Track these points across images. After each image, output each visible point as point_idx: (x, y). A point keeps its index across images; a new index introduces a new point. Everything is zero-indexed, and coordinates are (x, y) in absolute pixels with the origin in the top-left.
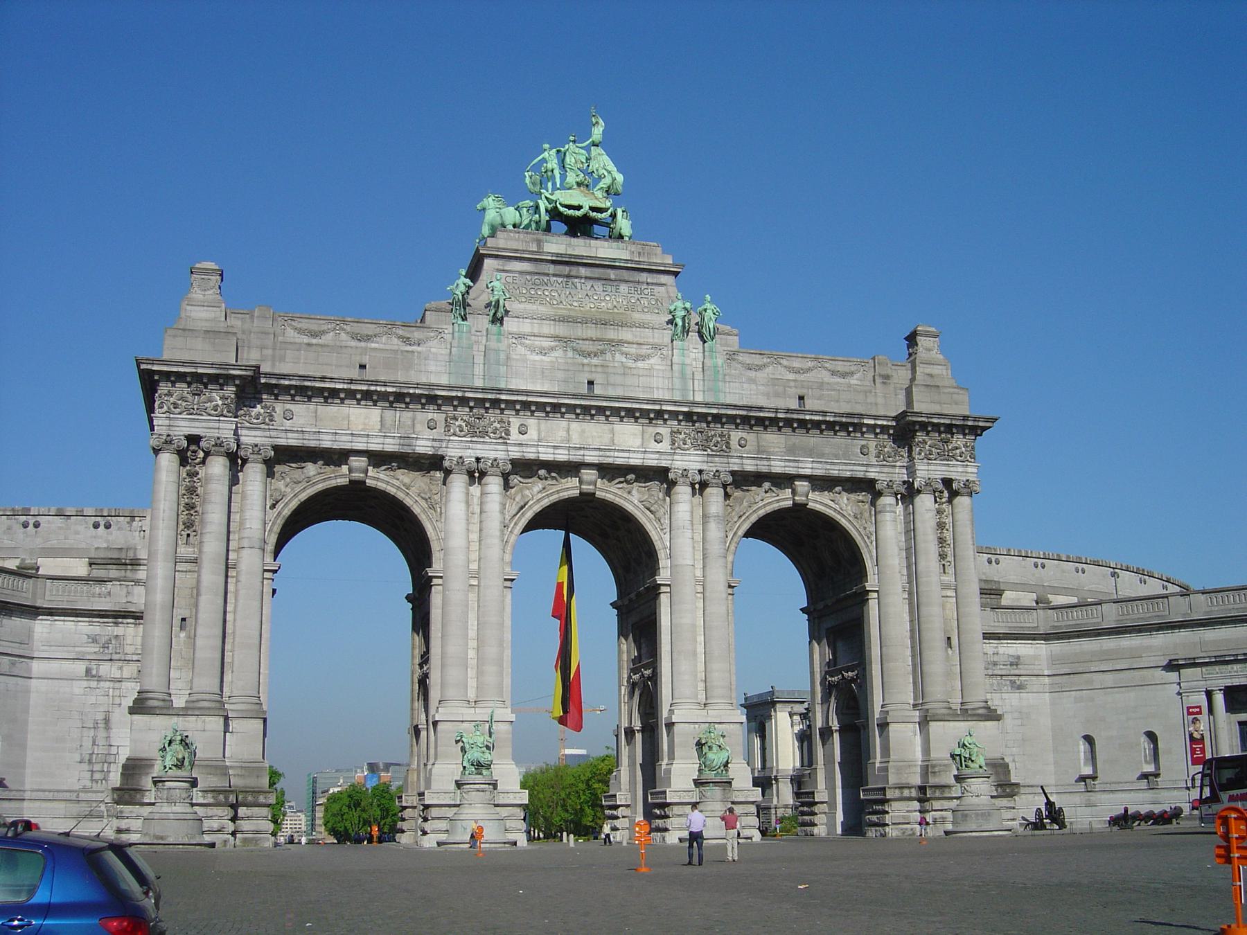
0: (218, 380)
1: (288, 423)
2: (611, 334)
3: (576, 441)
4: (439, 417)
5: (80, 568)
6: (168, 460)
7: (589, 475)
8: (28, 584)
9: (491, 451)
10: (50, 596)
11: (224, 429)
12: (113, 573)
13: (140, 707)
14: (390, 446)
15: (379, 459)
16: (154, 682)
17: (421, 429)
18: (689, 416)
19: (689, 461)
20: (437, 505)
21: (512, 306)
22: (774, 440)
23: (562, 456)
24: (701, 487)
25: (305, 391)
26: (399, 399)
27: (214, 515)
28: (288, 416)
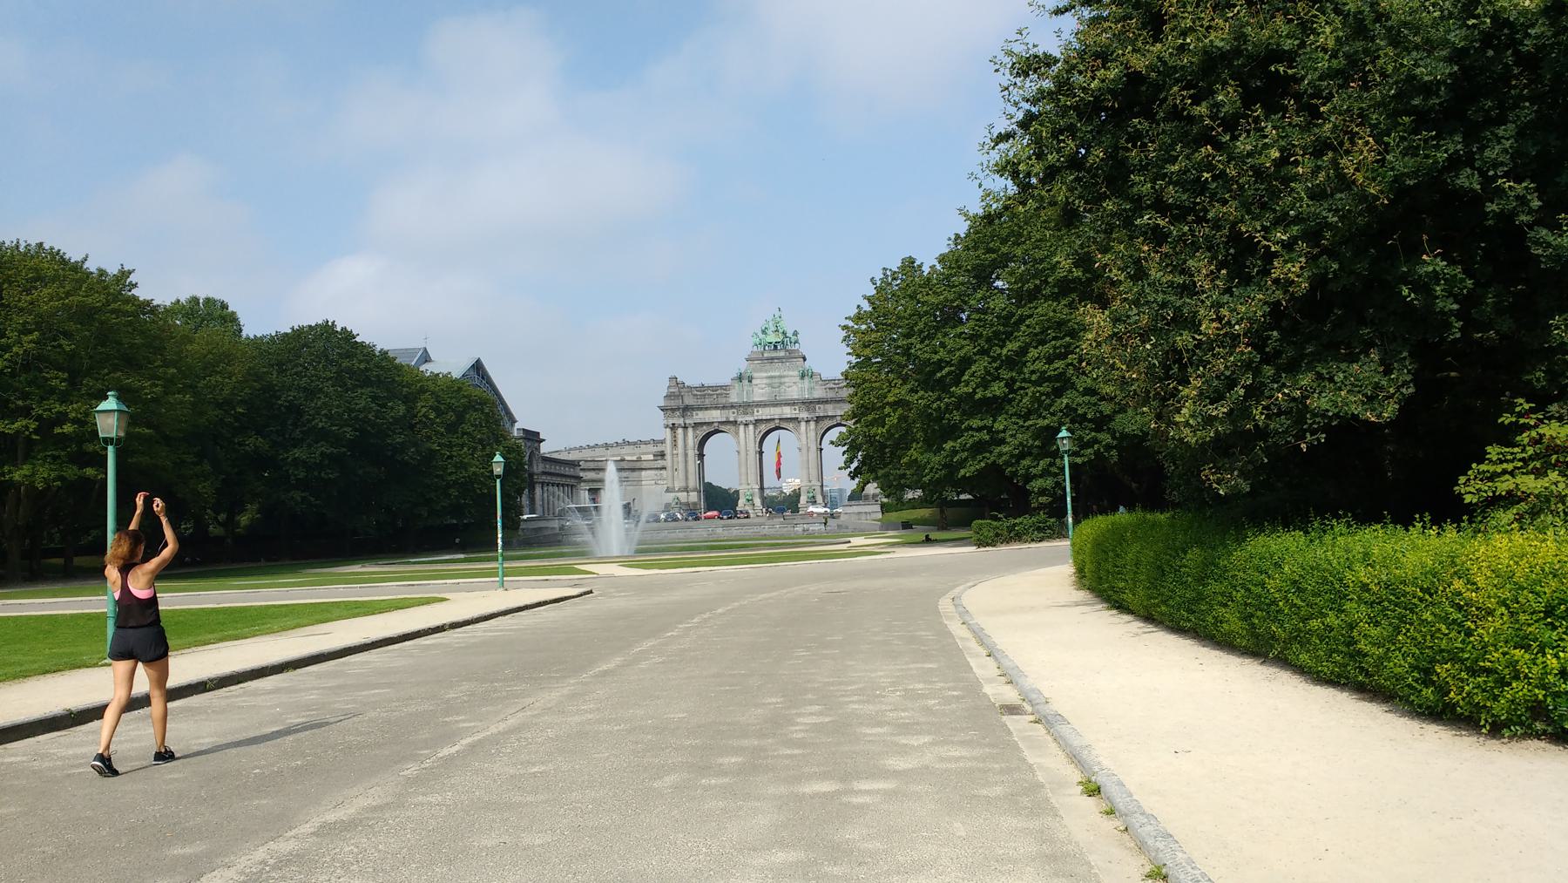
0: (679, 409)
1: (697, 417)
2: (783, 380)
3: (772, 412)
4: (735, 411)
5: (651, 457)
7: (777, 421)
8: (639, 463)
9: (749, 418)
10: (644, 465)
11: (681, 421)
12: (659, 458)
14: (724, 420)
16: (670, 485)
17: (731, 414)
19: (804, 415)
21: (755, 375)
23: (769, 417)
24: (808, 421)
25: (700, 409)
26: (724, 408)
28: (697, 414)
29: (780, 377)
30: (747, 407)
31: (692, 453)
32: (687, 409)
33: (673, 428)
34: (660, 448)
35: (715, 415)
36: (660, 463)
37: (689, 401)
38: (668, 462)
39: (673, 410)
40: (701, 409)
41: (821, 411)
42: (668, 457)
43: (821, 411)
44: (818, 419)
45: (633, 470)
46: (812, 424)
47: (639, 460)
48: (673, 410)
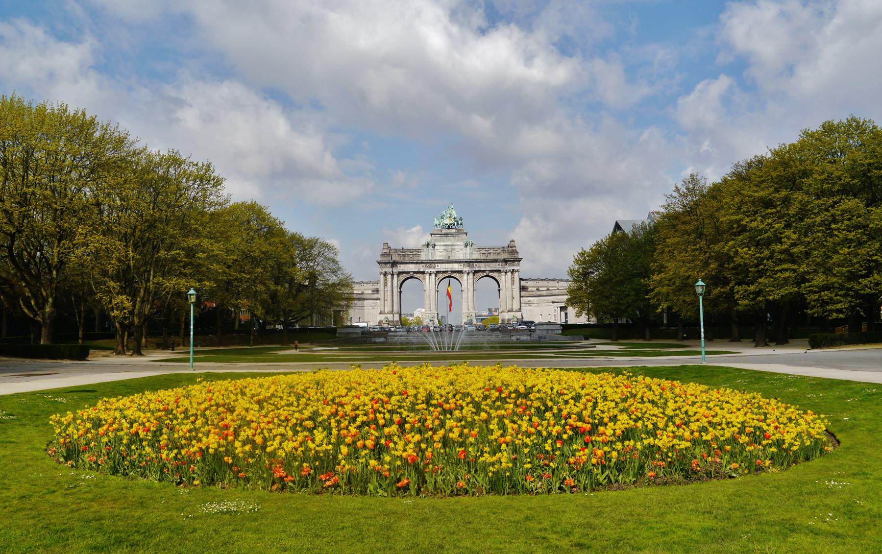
0: (389, 263)
5: (370, 292)
6: (382, 276)
10: (366, 297)
11: (390, 270)
13: (381, 313)
15: (415, 272)
16: (382, 310)
18: (466, 262)
19: (467, 269)
20: (424, 279)
21: (436, 244)
22: (482, 264)
24: (468, 274)
26: (417, 263)
27: (389, 284)
29: (452, 245)
30: (431, 263)
31: (395, 290)
32: (394, 264)
33: (385, 274)
34: (376, 287)
35: (412, 268)
36: (376, 296)
37: (396, 258)
38: (381, 295)
39: (386, 263)
40: (403, 263)
41: (477, 267)
42: (381, 292)
43: (477, 267)
44: (476, 272)
45: (360, 299)
46: (471, 275)
47: (363, 294)
48: (386, 263)
